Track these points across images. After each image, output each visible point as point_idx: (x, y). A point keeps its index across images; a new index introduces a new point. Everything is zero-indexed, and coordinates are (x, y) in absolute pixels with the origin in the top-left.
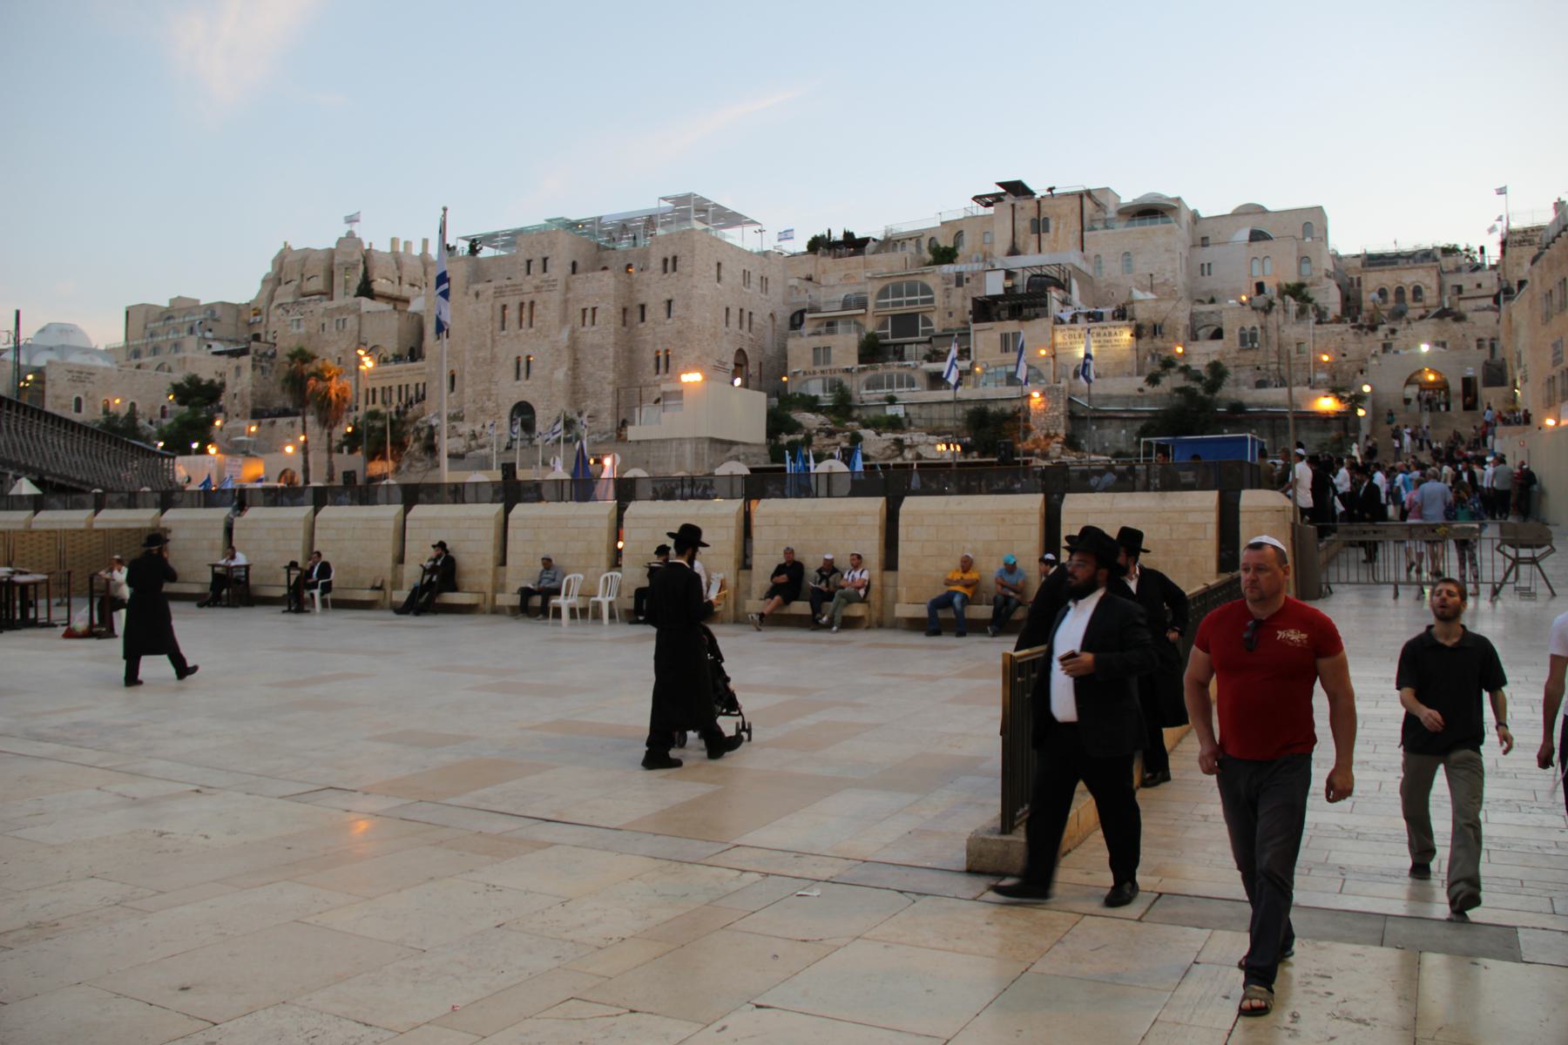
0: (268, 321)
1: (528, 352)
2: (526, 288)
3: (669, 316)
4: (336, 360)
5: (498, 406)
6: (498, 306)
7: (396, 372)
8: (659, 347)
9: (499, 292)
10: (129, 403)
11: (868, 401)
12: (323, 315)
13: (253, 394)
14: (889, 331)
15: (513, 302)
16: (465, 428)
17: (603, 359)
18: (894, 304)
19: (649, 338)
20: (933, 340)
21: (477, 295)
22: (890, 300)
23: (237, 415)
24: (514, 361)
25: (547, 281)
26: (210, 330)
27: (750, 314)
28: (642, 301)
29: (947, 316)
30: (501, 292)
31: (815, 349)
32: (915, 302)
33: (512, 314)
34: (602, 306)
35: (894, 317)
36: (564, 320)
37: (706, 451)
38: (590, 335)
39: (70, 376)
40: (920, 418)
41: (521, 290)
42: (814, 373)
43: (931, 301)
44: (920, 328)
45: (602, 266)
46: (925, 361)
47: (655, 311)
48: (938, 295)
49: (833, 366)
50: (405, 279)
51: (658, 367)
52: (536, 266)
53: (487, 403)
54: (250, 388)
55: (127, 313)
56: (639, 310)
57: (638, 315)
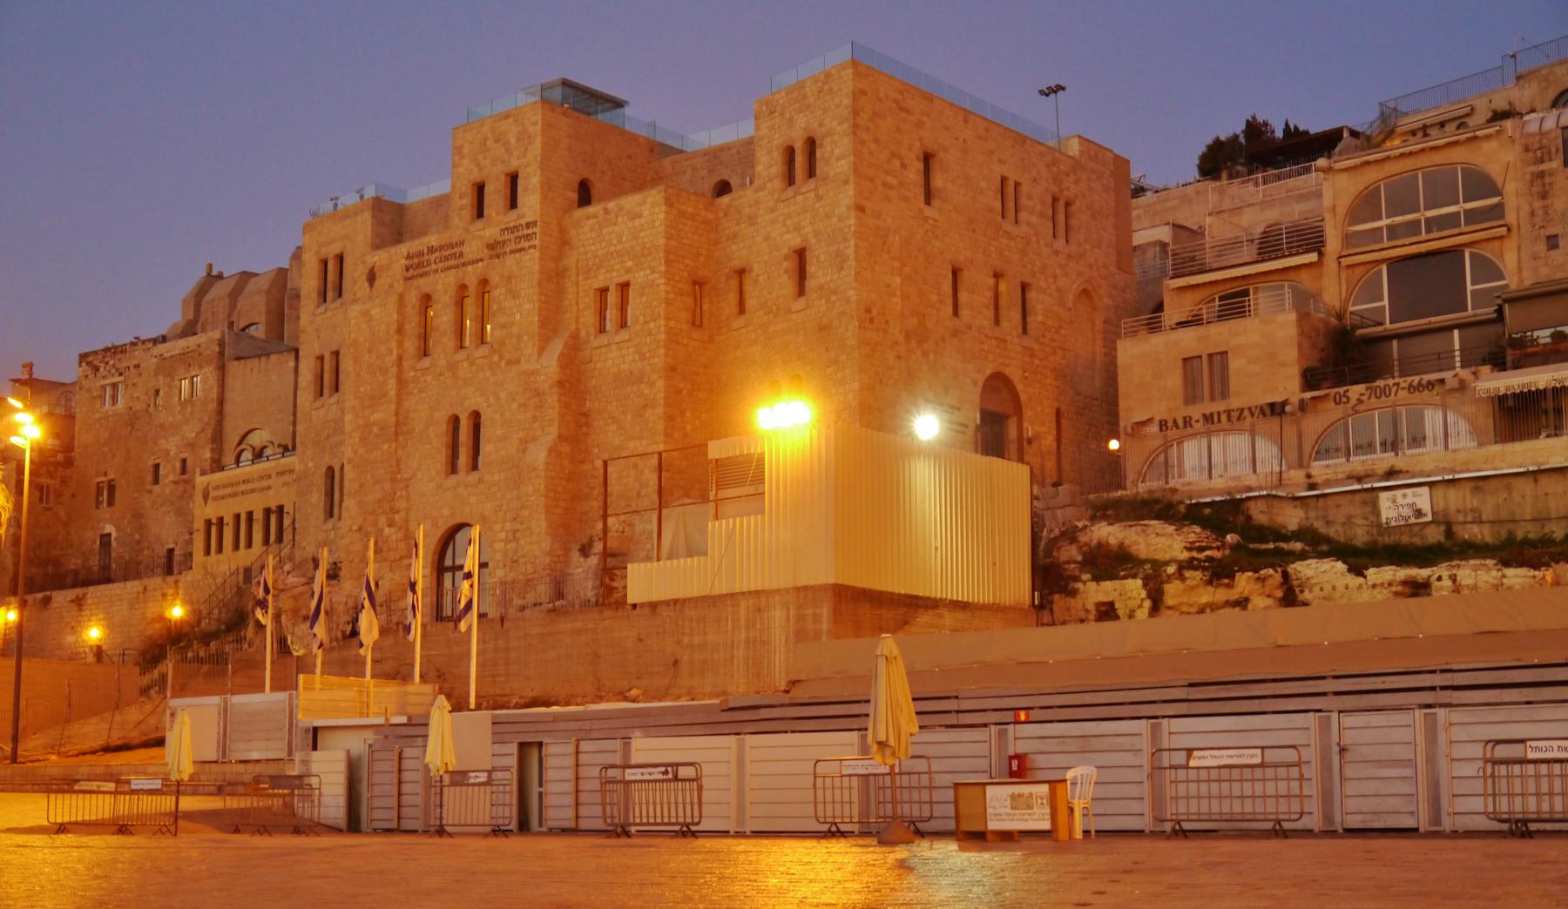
1: (475, 401)
2: (472, 249)
3: (801, 291)
4: (178, 465)
6: (413, 299)
7: (261, 478)
11: (1328, 483)
12: (156, 373)
14: (1386, 302)
15: (442, 284)
17: (645, 407)
18: (1393, 231)
20: (1506, 307)
22: (1384, 222)
24: (443, 427)
25: (516, 228)
27: (1024, 288)
28: (736, 264)
29: (1541, 247)
31: (1185, 360)
32: (1452, 220)
33: (442, 316)
34: (639, 278)
35: (1393, 263)
36: (550, 323)
37: (825, 626)
40: (1479, 521)
41: (461, 254)
42: (1187, 421)
43: (1497, 212)
44: (1469, 287)
46: (1485, 370)
48: (1515, 199)
49: (1235, 403)
53: (387, 531)
56: (734, 282)
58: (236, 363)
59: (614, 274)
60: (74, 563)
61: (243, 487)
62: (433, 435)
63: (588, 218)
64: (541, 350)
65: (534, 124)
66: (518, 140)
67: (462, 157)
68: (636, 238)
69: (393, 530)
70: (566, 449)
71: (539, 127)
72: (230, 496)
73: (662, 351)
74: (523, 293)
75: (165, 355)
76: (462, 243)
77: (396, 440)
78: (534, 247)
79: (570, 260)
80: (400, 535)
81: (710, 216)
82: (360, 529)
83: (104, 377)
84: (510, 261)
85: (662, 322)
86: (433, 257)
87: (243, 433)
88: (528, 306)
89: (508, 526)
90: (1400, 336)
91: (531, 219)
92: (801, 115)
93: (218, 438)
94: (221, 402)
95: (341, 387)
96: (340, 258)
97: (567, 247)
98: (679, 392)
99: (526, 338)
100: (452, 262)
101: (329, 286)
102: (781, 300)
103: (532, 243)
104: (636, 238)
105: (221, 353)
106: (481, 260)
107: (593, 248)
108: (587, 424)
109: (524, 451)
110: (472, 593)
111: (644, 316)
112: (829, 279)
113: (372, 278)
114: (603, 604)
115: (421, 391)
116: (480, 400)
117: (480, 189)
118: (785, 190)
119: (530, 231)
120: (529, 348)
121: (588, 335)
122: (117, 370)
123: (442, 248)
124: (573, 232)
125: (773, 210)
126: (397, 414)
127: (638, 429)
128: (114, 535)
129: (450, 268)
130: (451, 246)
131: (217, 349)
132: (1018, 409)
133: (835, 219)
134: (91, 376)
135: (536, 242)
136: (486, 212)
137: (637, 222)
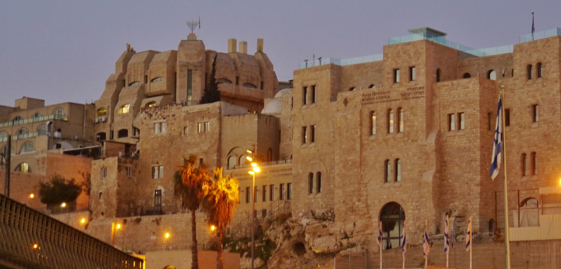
0: (113, 121)
1: (396, 155)
2: (394, 95)
3: (534, 120)
5: (367, 206)
6: (366, 112)
8: (525, 150)
9: (367, 99)
12: (185, 119)
13: (118, 193)
15: (381, 108)
16: (336, 227)
17: (472, 161)
19: (515, 141)
21: (346, 102)
23: (103, 214)
26: (59, 130)
30: (368, 99)
36: (430, 127)
41: (389, 97)
45: (463, 73)
50: (243, 79)
51: (523, 169)
53: (357, 203)
54: (116, 188)
58: (227, 117)
59: (456, 109)
60: (141, 202)
62: (377, 167)
63: (444, 86)
64: (427, 136)
65: (423, 48)
66: (415, 54)
67: (388, 58)
68: (466, 96)
69: (360, 203)
70: (438, 175)
71: (424, 50)
73: (479, 140)
74: (418, 114)
75: (189, 112)
76: (389, 92)
77: (360, 168)
78: (423, 97)
79: (436, 102)
80: (364, 205)
81: (493, 87)
82: (344, 202)
83: (155, 119)
84: (412, 101)
85: (479, 129)
86: (375, 97)
87: (232, 148)
88: (421, 120)
89: (414, 204)
91: (421, 86)
92: (535, 54)
93: (219, 151)
94: (220, 134)
97: (434, 97)
98: (484, 155)
99: (420, 132)
100: (385, 99)
102: (526, 123)
103: (422, 95)
104: (466, 96)
105: (220, 113)
106: (399, 100)
107: (446, 98)
108: (445, 166)
109: (421, 175)
110: (470, 239)
111: (470, 126)
112: (548, 117)
114: (496, 241)
115: (371, 149)
116: (400, 154)
118: (527, 81)
119: (421, 90)
120: (422, 136)
121: (445, 131)
122: (162, 117)
123: (379, 93)
124: (437, 91)
125: (522, 88)
126: (360, 158)
127: (468, 169)
128: (163, 191)
129: (384, 102)
130: (384, 93)
131: (218, 111)
133: (551, 95)
134: (148, 118)
137: (467, 90)
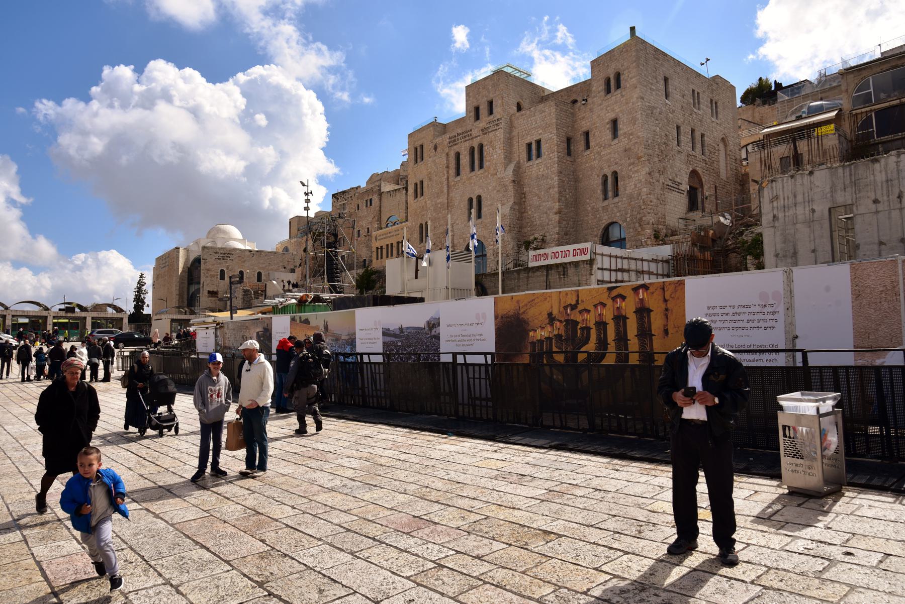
1: (478, 192)
2: (475, 132)
4: (366, 230)
7: (396, 231)
10: (256, 273)
15: (463, 148)
27: (702, 136)
28: (584, 129)
30: (454, 141)
33: (465, 160)
34: (544, 137)
36: (508, 159)
38: (536, 168)
39: (216, 256)
41: (471, 135)
47: (601, 135)
52: (483, 111)
55: (290, 222)
57: (582, 143)
59: (534, 136)
61: (389, 235)
62: (462, 206)
64: (505, 168)
70: (517, 207)
72: (385, 238)
76: (471, 130)
79: (515, 133)
84: (491, 135)
85: (556, 153)
86: (459, 137)
90: (883, 143)
93: (380, 219)
94: (380, 207)
95: (424, 194)
96: (422, 146)
98: (563, 182)
99: (499, 165)
100: (467, 138)
101: (418, 157)
102: (606, 141)
104: (543, 121)
106: (479, 136)
108: (525, 197)
111: (548, 152)
112: (628, 129)
113: (436, 148)
115: (456, 189)
116: (481, 191)
117: (477, 109)
118: (605, 96)
120: (500, 168)
121: (524, 162)
125: (601, 105)
127: (547, 197)
129: (466, 141)
130: (467, 132)
132: (702, 185)
135: (502, 126)
136: (480, 117)
137: (543, 114)
